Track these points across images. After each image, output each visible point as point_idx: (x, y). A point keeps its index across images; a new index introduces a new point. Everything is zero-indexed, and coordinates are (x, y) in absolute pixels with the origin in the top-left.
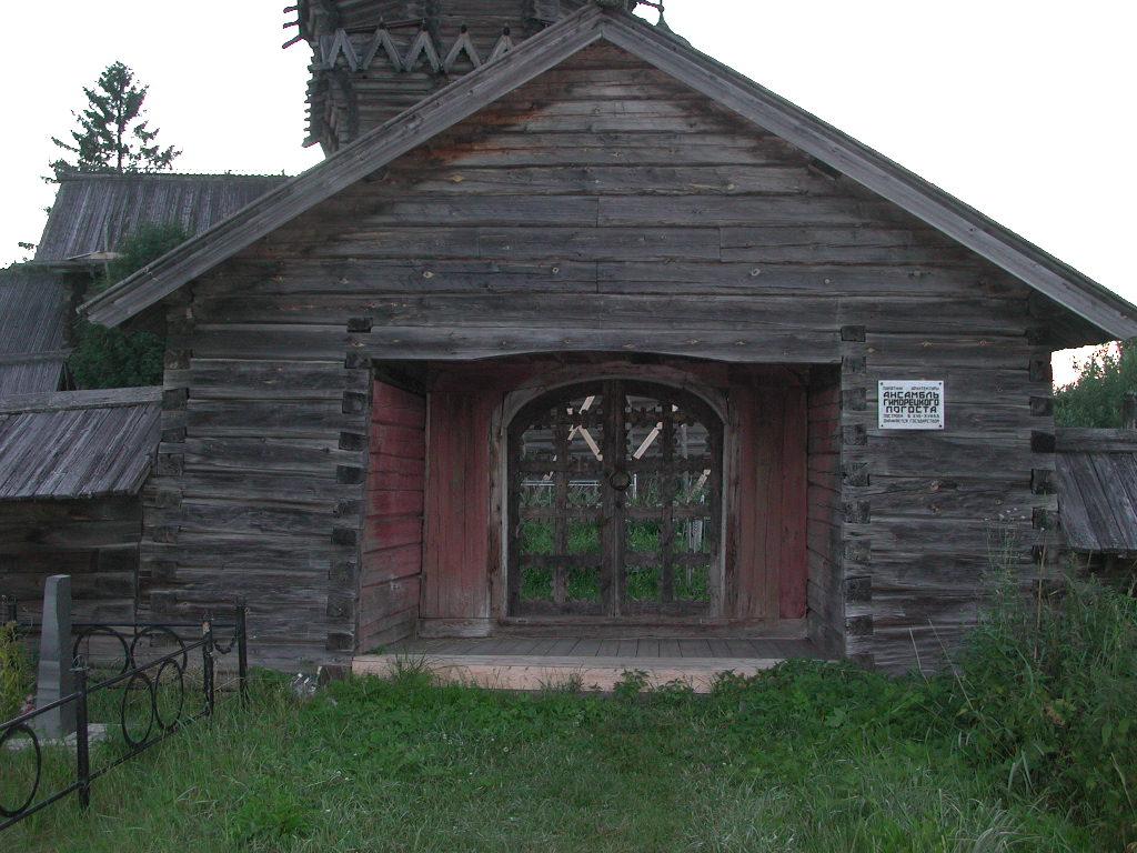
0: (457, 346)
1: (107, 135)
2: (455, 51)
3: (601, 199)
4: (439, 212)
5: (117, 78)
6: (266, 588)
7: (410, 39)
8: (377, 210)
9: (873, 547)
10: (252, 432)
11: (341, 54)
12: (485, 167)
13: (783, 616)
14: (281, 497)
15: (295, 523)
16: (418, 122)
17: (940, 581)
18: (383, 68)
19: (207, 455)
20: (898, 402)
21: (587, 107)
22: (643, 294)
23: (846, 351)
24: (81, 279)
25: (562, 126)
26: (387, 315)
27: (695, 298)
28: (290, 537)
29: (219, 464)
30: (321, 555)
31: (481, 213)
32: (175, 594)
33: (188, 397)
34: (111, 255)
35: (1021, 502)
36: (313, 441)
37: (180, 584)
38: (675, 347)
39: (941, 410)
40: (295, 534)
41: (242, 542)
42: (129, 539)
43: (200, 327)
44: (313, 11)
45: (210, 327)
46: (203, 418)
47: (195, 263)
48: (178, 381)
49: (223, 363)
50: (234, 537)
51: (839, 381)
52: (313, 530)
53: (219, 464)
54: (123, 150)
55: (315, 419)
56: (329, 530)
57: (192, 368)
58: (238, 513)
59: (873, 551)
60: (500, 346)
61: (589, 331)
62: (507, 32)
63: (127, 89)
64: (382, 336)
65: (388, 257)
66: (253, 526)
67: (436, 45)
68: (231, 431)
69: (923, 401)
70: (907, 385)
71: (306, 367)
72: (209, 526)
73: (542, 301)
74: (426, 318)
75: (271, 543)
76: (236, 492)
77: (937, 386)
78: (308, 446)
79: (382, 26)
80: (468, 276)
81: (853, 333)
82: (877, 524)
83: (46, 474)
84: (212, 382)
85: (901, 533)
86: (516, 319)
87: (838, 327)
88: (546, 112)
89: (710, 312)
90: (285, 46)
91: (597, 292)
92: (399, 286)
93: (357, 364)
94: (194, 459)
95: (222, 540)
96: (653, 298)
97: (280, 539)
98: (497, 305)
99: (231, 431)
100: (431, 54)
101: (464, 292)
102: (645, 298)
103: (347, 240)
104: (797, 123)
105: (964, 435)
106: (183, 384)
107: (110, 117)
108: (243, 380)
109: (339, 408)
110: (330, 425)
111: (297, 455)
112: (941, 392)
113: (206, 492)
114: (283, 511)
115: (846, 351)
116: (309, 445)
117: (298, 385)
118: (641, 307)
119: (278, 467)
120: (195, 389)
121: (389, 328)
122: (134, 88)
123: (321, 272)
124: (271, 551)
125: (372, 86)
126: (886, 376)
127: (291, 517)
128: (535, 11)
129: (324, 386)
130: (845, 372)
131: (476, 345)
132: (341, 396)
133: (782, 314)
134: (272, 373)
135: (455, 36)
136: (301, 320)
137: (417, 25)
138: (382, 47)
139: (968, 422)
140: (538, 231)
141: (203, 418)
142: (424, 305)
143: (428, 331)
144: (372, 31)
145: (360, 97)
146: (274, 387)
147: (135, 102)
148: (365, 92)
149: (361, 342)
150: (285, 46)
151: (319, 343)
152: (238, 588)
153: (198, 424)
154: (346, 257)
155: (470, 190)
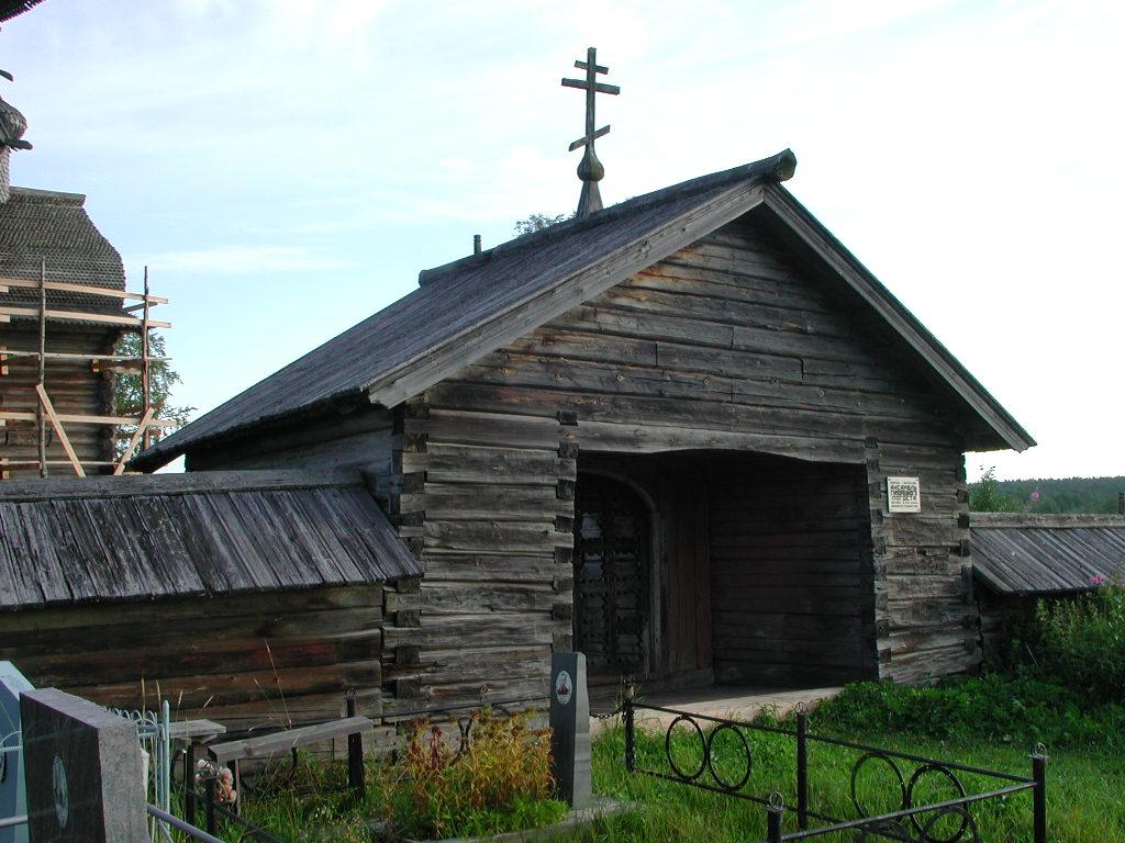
0: (642, 441)
3: (736, 328)
6: (500, 665)
9: (890, 598)
10: (483, 516)
12: (660, 291)
13: (698, 668)
14: (510, 577)
15: (521, 600)
16: (648, 247)
17: (921, 620)
22: (757, 405)
25: (710, 265)
26: (588, 412)
27: (787, 411)
28: (518, 615)
30: (544, 630)
31: (658, 329)
32: (420, 679)
33: (426, 481)
35: (956, 562)
36: (534, 525)
37: (423, 668)
38: (778, 449)
39: (918, 497)
40: (522, 611)
41: (477, 622)
42: (368, 627)
43: (432, 411)
45: (443, 412)
46: (438, 502)
47: (469, 351)
48: (418, 464)
49: (458, 448)
50: (468, 618)
51: (866, 477)
52: (536, 608)
53: (458, 547)
55: (537, 504)
56: (549, 606)
57: (429, 452)
59: (890, 600)
60: (671, 443)
61: (725, 433)
64: (586, 430)
65: (590, 360)
66: (484, 606)
68: (466, 514)
71: (524, 455)
72: (448, 608)
73: (694, 405)
74: (616, 415)
75: (506, 621)
76: (470, 574)
77: (914, 481)
78: (530, 529)
80: (649, 381)
81: (871, 442)
82: (891, 581)
84: (449, 467)
85: (902, 587)
86: (680, 421)
87: (864, 437)
89: (796, 421)
91: (731, 402)
92: (599, 387)
93: (568, 454)
94: (433, 542)
95: (461, 621)
96: (763, 409)
97: (512, 619)
98: (664, 406)
99: (466, 514)
101: (643, 395)
102: (759, 409)
103: (558, 340)
104: (871, 288)
106: (421, 468)
108: (475, 464)
109: (552, 493)
110: (548, 509)
111: (521, 537)
112: (917, 486)
113: (442, 575)
114: (511, 590)
115: (868, 456)
116: (531, 527)
117: (522, 471)
118: (755, 415)
120: (433, 472)
121: (589, 424)
123: (539, 368)
124: (501, 629)
126: (896, 474)
127: (518, 596)
129: (543, 473)
131: (654, 440)
132: (556, 482)
133: (835, 425)
134: (501, 458)
136: (531, 412)
140: (695, 349)
141: (438, 502)
142: (620, 402)
146: (502, 473)
149: (572, 435)
151: (538, 432)
152: (476, 666)
153: (434, 507)
154: (558, 356)
155: (650, 308)
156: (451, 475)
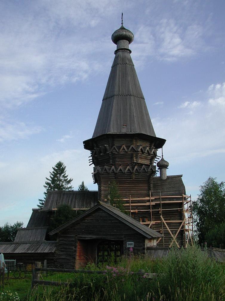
1: (57, 177)
2: (119, 169)
4: (84, 224)
5: (59, 165)
7: (111, 167)
8: (78, 223)
11: (98, 170)
18: (106, 173)
19: (61, 249)
20: (129, 244)
21: (98, 213)
23: (124, 239)
24: (51, 213)
26: (79, 234)
29: (62, 250)
34: (56, 209)
44: (95, 161)
46: (61, 245)
53: (62, 250)
54: (61, 180)
58: (64, 255)
60: (90, 238)
62: (129, 165)
63: (61, 168)
67: (116, 168)
69: (132, 244)
70: (130, 243)
77: (133, 243)
79: (105, 165)
83: (45, 250)
88: (95, 214)
90: (90, 165)
98: (90, 234)
100: (115, 170)
105: (136, 248)
107: (58, 173)
108: (65, 241)
115: (124, 239)
116: (71, 248)
119: (68, 250)
122: (63, 167)
125: (104, 176)
128: (134, 161)
130: (124, 241)
135: (119, 166)
137: (112, 164)
138: (105, 169)
139: (136, 247)
141: (61, 245)
143: (83, 236)
144: (104, 166)
145: (102, 178)
147: (63, 169)
148: (102, 177)
150: (90, 165)
151: (73, 237)
156: (62, 242)
